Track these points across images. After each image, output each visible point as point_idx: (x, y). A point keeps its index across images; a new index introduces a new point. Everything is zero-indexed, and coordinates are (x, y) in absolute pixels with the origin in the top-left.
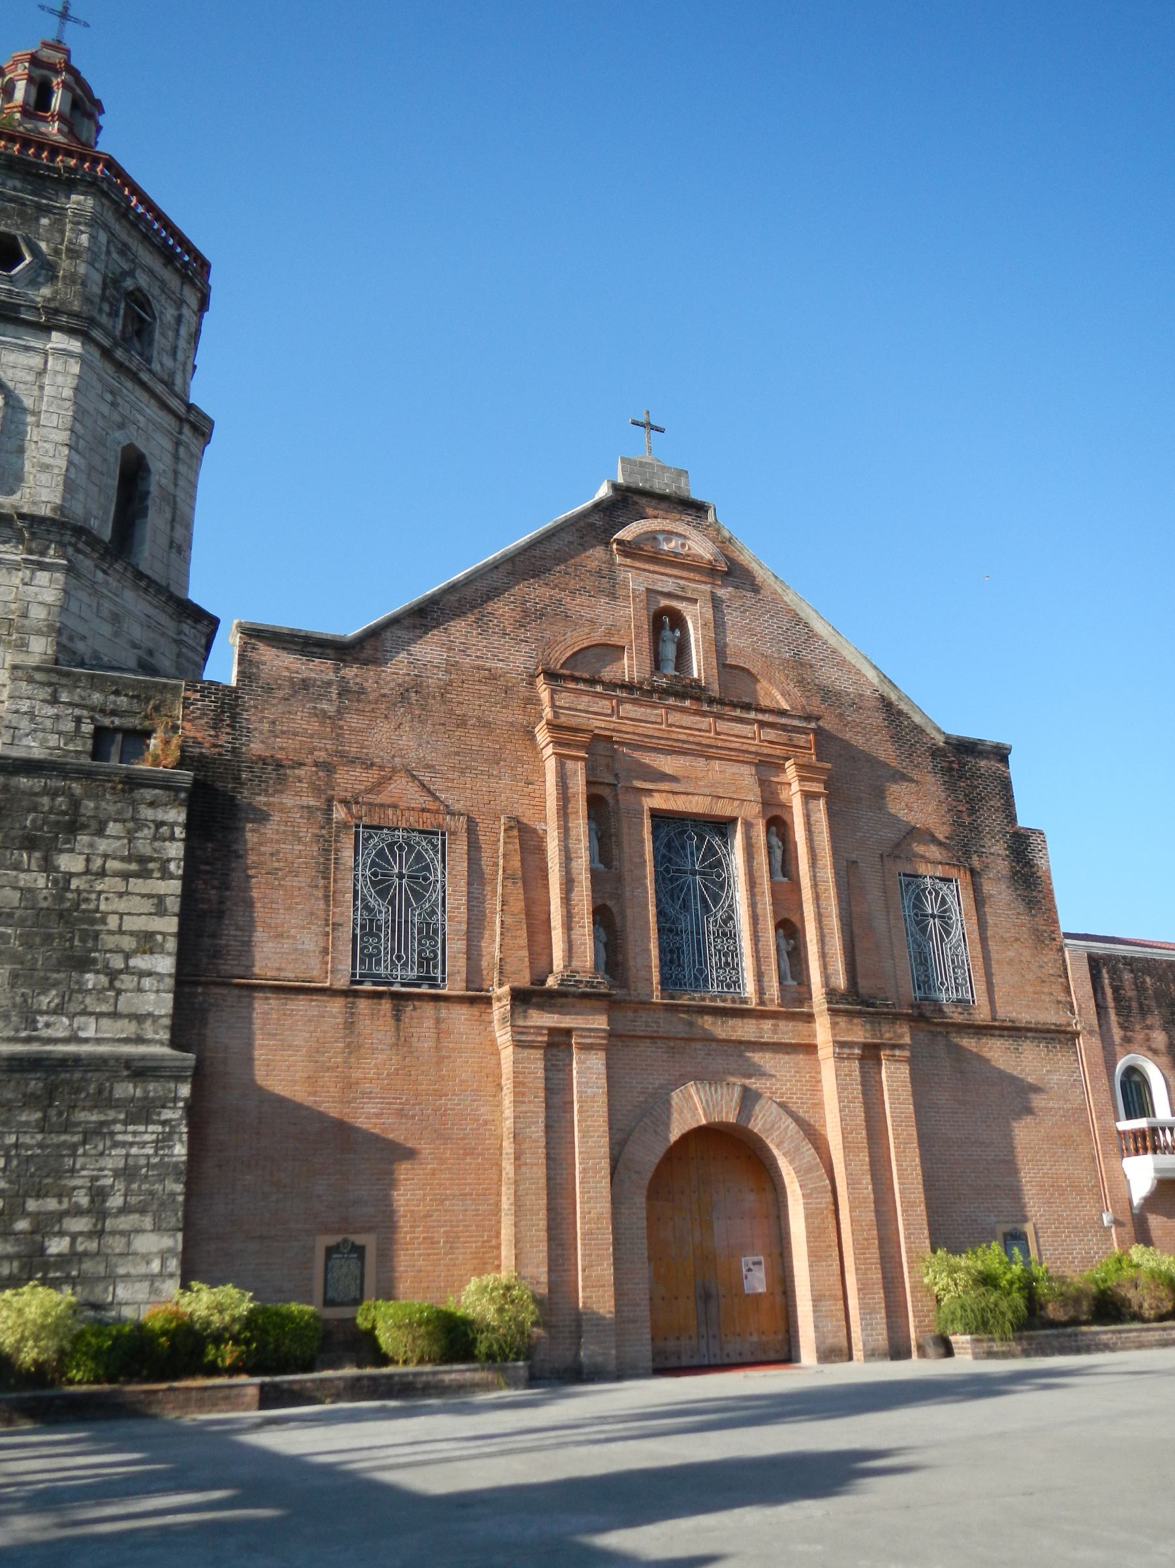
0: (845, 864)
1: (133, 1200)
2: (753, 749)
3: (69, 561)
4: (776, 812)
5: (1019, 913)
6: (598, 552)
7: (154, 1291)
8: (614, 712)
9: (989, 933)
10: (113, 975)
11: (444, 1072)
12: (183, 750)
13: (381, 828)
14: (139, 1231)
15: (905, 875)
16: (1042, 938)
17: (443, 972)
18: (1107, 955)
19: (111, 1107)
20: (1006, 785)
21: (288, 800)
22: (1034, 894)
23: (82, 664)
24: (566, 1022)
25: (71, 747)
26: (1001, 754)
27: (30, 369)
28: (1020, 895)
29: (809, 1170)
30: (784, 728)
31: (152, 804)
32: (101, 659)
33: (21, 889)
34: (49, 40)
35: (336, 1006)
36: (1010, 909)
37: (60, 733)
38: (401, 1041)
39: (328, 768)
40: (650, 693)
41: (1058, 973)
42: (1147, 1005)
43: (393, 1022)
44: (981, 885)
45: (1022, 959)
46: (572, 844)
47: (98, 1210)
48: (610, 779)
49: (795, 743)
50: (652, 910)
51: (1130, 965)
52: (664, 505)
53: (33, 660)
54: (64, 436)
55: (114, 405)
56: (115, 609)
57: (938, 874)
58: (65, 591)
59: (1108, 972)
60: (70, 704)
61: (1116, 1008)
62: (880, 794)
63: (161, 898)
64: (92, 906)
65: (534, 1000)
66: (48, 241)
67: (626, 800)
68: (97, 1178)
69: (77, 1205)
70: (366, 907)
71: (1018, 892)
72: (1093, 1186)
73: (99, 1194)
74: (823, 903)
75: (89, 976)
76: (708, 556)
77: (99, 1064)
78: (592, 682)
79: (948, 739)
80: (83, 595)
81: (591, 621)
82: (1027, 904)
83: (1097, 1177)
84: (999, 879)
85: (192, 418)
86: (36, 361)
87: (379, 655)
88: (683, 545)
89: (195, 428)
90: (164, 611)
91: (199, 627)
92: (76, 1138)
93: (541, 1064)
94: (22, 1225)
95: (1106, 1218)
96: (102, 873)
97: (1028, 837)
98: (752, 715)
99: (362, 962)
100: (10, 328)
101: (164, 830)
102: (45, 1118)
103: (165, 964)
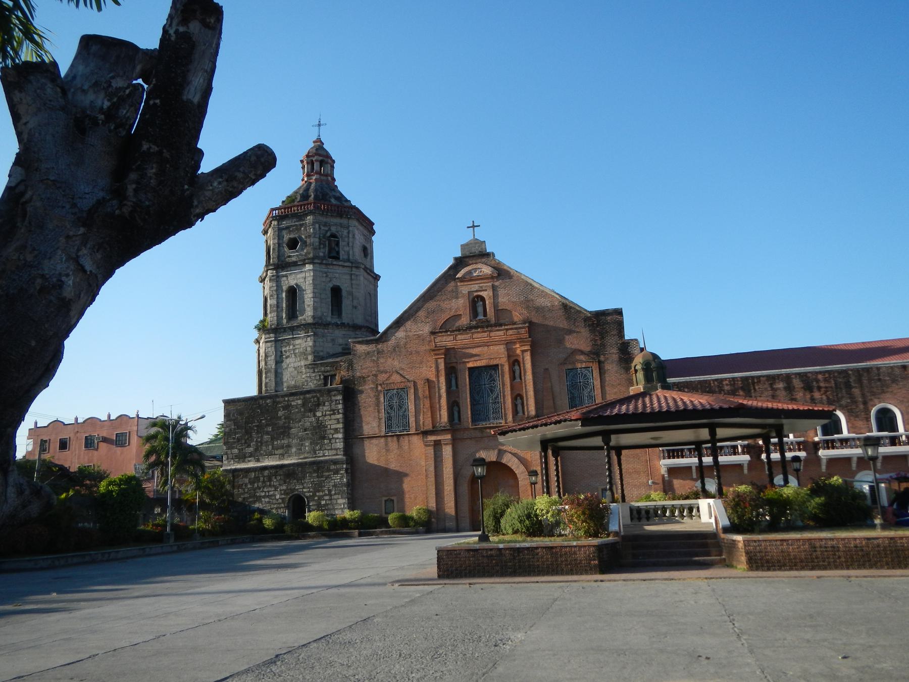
0: (543, 370)
1: (336, 492)
2: (504, 339)
3: (314, 332)
4: (515, 358)
6: (452, 284)
7: (343, 512)
8: (455, 339)
9: (606, 384)
10: (330, 440)
11: (411, 454)
12: (341, 378)
13: (390, 390)
14: (338, 499)
15: (568, 369)
17: (409, 427)
19: (331, 471)
20: (620, 326)
21: (367, 387)
23: (322, 359)
24: (439, 438)
25: (319, 383)
26: (619, 312)
27: (303, 278)
29: (521, 473)
30: (516, 329)
31: (334, 396)
32: (329, 353)
33: (310, 422)
34: (315, 139)
35: (382, 440)
36: (616, 373)
37: (316, 380)
38: (400, 447)
39: (376, 376)
40: (466, 330)
43: (396, 441)
44: (604, 366)
45: (621, 391)
46: (440, 385)
47: (330, 495)
48: (455, 361)
49: (521, 332)
50: (469, 400)
52: (475, 258)
53: (309, 362)
54: (311, 295)
55: (327, 276)
56: (332, 338)
57: (583, 366)
58: (314, 341)
60: (318, 372)
62: (561, 341)
63: (338, 419)
64: (324, 424)
65: (429, 433)
66: (304, 235)
67: (460, 367)
68: (329, 487)
69: (326, 494)
70: (388, 413)
73: (330, 491)
74: (528, 387)
75: (325, 441)
76: (490, 273)
77: (326, 462)
78: (446, 332)
79: (590, 312)
80: (320, 340)
81: (450, 309)
83: (648, 468)
85: (354, 265)
86: (303, 275)
87: (387, 339)
88: (481, 271)
89: (357, 267)
90: (349, 331)
91: (362, 330)
92: (324, 479)
93: (433, 450)
94: (316, 498)
96: (326, 415)
97: (629, 343)
98: (503, 327)
99: (388, 428)
100: (297, 267)
101: (338, 402)
102: (318, 475)
103: (340, 436)
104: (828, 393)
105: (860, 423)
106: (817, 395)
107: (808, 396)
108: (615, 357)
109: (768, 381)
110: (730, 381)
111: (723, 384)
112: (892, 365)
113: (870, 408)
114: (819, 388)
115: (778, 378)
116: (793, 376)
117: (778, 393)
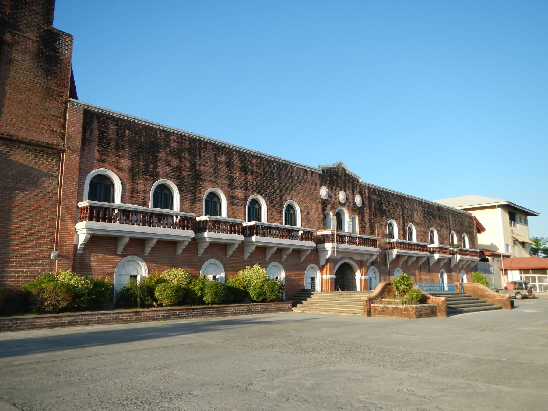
5: (36, 76)
16: (51, 94)
18: (101, 113)
22: (53, 68)
28: (40, 66)
41: (59, 115)
42: (121, 144)
45: (31, 101)
51: (116, 121)
59: (98, 122)
61: (98, 142)
71: (40, 64)
72: (48, 236)
82: (45, 72)
84: (26, 52)
95: (53, 255)
97: (59, 36)
104: (258, 179)
105: (276, 215)
106: (250, 178)
107: (243, 178)
108: (32, 46)
109: (214, 151)
110: (177, 138)
111: (170, 139)
112: (300, 167)
113: (284, 202)
114: (252, 172)
115: (222, 150)
116: (234, 153)
117: (220, 166)
